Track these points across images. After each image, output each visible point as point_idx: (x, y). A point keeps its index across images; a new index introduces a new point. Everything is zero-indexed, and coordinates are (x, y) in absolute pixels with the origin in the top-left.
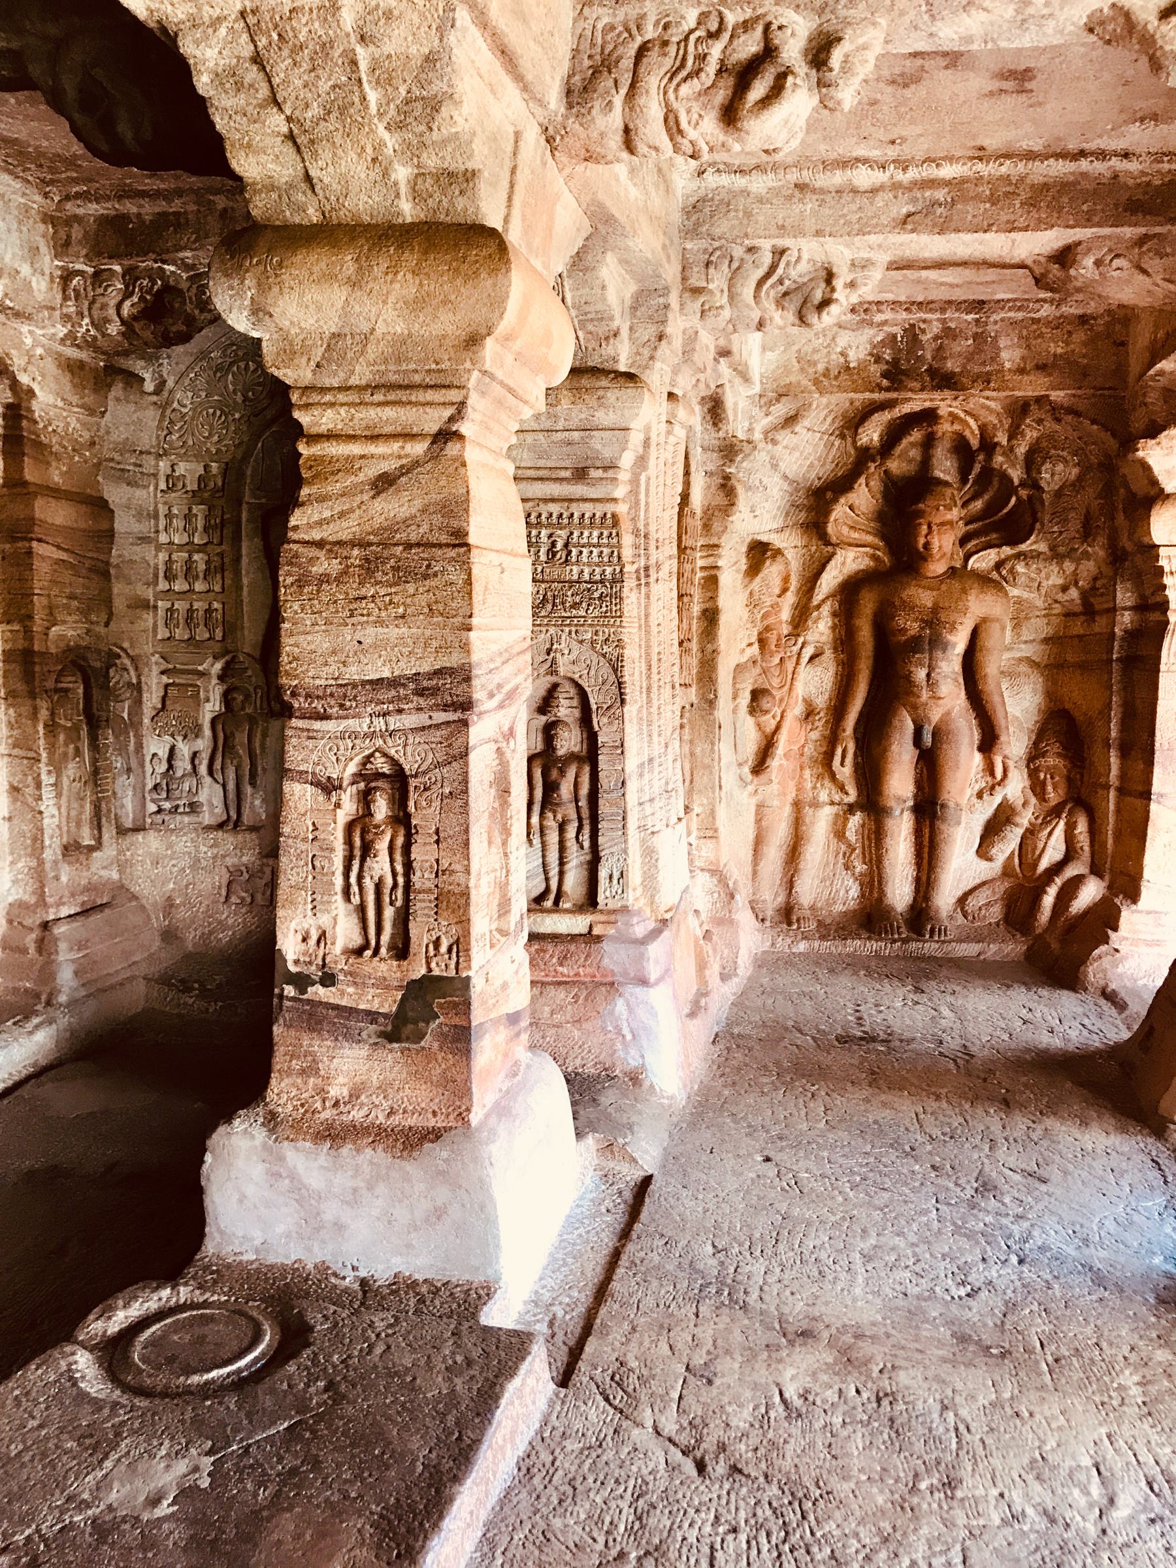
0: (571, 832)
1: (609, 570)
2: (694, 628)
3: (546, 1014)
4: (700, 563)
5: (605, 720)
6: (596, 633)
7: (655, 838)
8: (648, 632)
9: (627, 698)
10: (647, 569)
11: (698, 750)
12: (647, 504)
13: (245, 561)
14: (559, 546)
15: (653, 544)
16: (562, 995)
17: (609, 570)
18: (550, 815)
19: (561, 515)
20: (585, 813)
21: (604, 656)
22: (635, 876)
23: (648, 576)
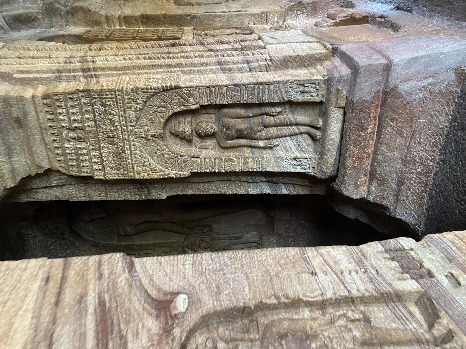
0: (271, 120)
1: (84, 101)
2: (153, 29)
3: (403, 141)
4: (118, 27)
5: (191, 100)
6: (130, 108)
7: (275, 59)
8: (128, 68)
9: (173, 84)
10: (83, 70)
11: (219, 25)
12: (38, 72)
13: (143, 242)
14: (72, 134)
15: (69, 66)
16: (390, 130)
17: (84, 101)
18: (258, 134)
19: (53, 134)
20: (257, 111)
21: (145, 102)
22: (302, 74)
23: (89, 70)
